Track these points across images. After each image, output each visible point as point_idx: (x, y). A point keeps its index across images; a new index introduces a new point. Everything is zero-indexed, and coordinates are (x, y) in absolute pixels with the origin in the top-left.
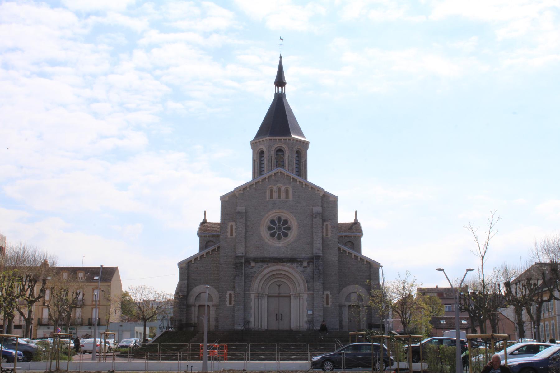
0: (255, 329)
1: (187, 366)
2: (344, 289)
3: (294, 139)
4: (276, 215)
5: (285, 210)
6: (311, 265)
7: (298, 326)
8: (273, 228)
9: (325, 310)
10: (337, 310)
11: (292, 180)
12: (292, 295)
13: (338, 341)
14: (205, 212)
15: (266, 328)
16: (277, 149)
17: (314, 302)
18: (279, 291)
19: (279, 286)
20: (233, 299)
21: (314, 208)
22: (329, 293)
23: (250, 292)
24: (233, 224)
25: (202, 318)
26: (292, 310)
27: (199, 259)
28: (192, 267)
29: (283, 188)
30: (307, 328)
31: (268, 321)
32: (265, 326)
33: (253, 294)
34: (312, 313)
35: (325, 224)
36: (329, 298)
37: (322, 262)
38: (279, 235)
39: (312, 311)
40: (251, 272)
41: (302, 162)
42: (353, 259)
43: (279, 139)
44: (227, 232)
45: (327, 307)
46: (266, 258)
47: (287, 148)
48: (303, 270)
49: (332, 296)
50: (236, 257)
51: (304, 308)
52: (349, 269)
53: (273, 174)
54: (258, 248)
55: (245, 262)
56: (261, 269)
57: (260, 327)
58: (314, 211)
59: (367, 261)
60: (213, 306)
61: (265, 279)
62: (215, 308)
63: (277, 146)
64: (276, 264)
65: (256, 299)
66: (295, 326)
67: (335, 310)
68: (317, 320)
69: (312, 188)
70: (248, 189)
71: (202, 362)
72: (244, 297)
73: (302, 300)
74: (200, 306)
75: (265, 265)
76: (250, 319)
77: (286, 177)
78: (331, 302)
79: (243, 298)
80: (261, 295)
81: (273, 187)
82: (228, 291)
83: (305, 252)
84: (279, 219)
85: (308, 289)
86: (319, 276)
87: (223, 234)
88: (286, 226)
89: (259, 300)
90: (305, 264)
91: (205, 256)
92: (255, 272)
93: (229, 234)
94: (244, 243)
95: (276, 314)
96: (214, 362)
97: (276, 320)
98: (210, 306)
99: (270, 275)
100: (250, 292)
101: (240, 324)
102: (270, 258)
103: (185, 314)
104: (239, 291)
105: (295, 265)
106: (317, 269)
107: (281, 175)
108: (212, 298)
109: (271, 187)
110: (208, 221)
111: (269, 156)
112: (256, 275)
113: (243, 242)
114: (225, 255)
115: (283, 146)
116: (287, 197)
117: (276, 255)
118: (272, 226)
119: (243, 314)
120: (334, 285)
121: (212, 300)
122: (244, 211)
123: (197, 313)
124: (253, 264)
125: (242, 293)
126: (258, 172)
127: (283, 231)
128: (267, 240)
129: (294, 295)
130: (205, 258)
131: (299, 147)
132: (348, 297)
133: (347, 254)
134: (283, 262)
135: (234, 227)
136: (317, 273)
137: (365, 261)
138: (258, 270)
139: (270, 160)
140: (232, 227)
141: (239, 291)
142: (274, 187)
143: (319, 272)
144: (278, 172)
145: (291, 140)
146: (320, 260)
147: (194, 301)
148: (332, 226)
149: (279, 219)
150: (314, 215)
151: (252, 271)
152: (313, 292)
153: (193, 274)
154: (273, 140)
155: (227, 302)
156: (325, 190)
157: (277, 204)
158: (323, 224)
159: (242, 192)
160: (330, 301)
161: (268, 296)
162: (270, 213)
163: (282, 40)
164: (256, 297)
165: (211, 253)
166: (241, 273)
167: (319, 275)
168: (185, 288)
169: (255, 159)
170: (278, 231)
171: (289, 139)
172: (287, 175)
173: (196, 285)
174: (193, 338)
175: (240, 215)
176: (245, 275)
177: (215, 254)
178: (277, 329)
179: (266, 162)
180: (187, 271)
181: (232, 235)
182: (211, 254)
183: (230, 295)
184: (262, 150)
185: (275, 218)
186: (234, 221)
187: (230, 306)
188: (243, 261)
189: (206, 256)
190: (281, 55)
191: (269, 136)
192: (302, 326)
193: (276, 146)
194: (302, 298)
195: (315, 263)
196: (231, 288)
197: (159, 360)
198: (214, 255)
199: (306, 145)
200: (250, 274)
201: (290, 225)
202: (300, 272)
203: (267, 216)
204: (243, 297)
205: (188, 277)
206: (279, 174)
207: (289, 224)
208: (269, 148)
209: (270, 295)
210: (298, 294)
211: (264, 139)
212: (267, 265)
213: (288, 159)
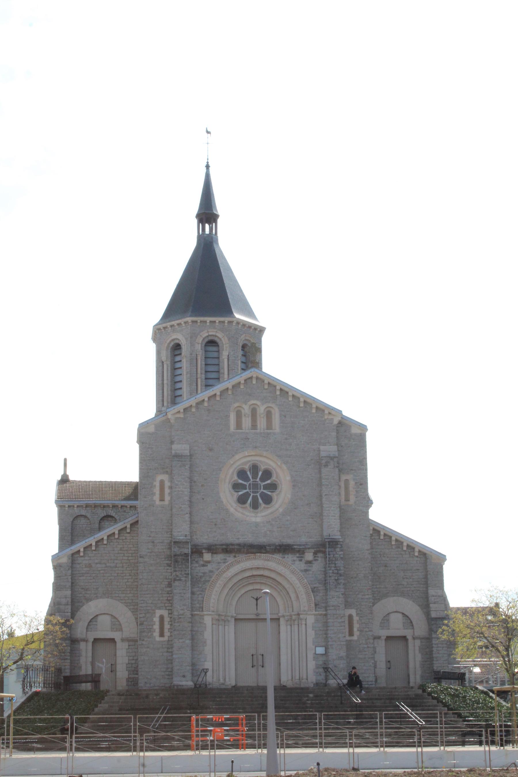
1: (232, 762)
2: (376, 605)
3: (239, 322)
4: (250, 461)
5: (267, 451)
6: (320, 559)
7: (297, 677)
8: (244, 487)
9: (349, 645)
10: (369, 646)
11: (278, 393)
12: (283, 616)
13: (403, 706)
14: (65, 460)
15: (233, 684)
16: (206, 340)
17: (327, 630)
18: (257, 610)
19: (257, 599)
20: (167, 626)
21: (322, 448)
22: (353, 612)
23: (202, 611)
24: (165, 477)
25: (100, 665)
26: (283, 646)
27: (93, 548)
28: (79, 564)
29: (261, 410)
30: (315, 682)
31: (236, 670)
32: (231, 682)
33: (207, 615)
34: (324, 652)
35: (344, 477)
36: (355, 622)
37: (342, 553)
38: (255, 499)
39: (324, 648)
40: (204, 573)
42: (394, 547)
44: (154, 494)
45: (350, 641)
46: (232, 545)
47: (226, 338)
48: (306, 568)
49: (360, 619)
50: (175, 542)
51: (308, 641)
52: (386, 566)
53: (243, 382)
54: (216, 524)
55: (192, 553)
56: (223, 567)
58: (323, 454)
59: (420, 551)
60: (123, 640)
61: (230, 585)
62: (126, 645)
63: (207, 334)
64: (252, 556)
66: (290, 678)
67: (366, 646)
68: (335, 666)
69: (317, 408)
70: (194, 410)
71: (265, 751)
72: (191, 622)
73: (304, 626)
74: (96, 640)
75: (230, 559)
77: (266, 387)
78: (358, 630)
79: (190, 625)
80: (223, 618)
81: (242, 407)
82: (157, 611)
83: (308, 532)
84: (255, 468)
85: (316, 605)
86: (336, 580)
87: (145, 497)
88: (269, 482)
89: (220, 627)
90: (309, 556)
91: (105, 542)
92: (211, 572)
93: (157, 497)
94: (188, 515)
95: (252, 655)
96: (217, 753)
97: (253, 667)
98: (116, 640)
99: (240, 577)
100: (202, 611)
101: (184, 676)
102: (239, 545)
103: (69, 658)
104: (182, 610)
105: (290, 558)
106: (333, 565)
107: (257, 382)
108: (120, 625)
109: (238, 407)
110: (71, 478)
111: (191, 354)
112: (213, 578)
113: (187, 514)
114: (151, 538)
115: (218, 334)
116: (269, 425)
117: (250, 539)
118: (240, 481)
119: (191, 656)
121: (121, 630)
122: (187, 453)
123: (90, 654)
124: (207, 556)
125: (188, 614)
126: (169, 384)
127: (262, 492)
128: (232, 510)
129: (286, 618)
130: (105, 546)
131: (247, 338)
132: (385, 621)
133: (382, 537)
134: (267, 552)
135: (167, 484)
136: (333, 573)
137: (417, 550)
138: (218, 569)
139: (193, 361)
140: (162, 483)
141: (182, 610)
142: (244, 406)
143: (336, 572)
144: (251, 378)
145: (234, 324)
146: (338, 547)
147: (85, 631)
148: (356, 483)
149: (255, 468)
150: (323, 462)
151: (206, 569)
152: (326, 610)
153: (81, 578)
154: (199, 324)
155: (155, 631)
156: (344, 414)
157: (250, 440)
158: (340, 480)
159: (182, 416)
160: (355, 629)
161: (236, 620)
162: (237, 457)
163: (209, 134)
164: (214, 622)
165: (116, 536)
166: (185, 574)
167: (336, 578)
168: (68, 605)
169: (164, 359)
170: (253, 492)
171: (230, 322)
172: (269, 383)
173: (88, 600)
174: (99, 705)
175: (178, 461)
176: (192, 578)
177: (124, 538)
179: (185, 364)
180: (70, 572)
181: (162, 499)
182: (118, 538)
183: (162, 618)
184: (177, 341)
185: (247, 467)
186: (167, 473)
187: (162, 639)
188: (188, 550)
189: (108, 542)
190: (208, 162)
191: (191, 316)
192: (305, 677)
194: (304, 622)
195: (329, 555)
196: (163, 605)
197: (71, 750)
198: (123, 540)
199: (260, 331)
200: (201, 576)
201: (276, 481)
202: (299, 571)
203: (232, 463)
204: (189, 622)
205: (72, 583)
206: (254, 382)
207: (274, 478)
208: (191, 337)
210: (295, 615)
211: (182, 321)
212: (236, 559)
213: (228, 359)
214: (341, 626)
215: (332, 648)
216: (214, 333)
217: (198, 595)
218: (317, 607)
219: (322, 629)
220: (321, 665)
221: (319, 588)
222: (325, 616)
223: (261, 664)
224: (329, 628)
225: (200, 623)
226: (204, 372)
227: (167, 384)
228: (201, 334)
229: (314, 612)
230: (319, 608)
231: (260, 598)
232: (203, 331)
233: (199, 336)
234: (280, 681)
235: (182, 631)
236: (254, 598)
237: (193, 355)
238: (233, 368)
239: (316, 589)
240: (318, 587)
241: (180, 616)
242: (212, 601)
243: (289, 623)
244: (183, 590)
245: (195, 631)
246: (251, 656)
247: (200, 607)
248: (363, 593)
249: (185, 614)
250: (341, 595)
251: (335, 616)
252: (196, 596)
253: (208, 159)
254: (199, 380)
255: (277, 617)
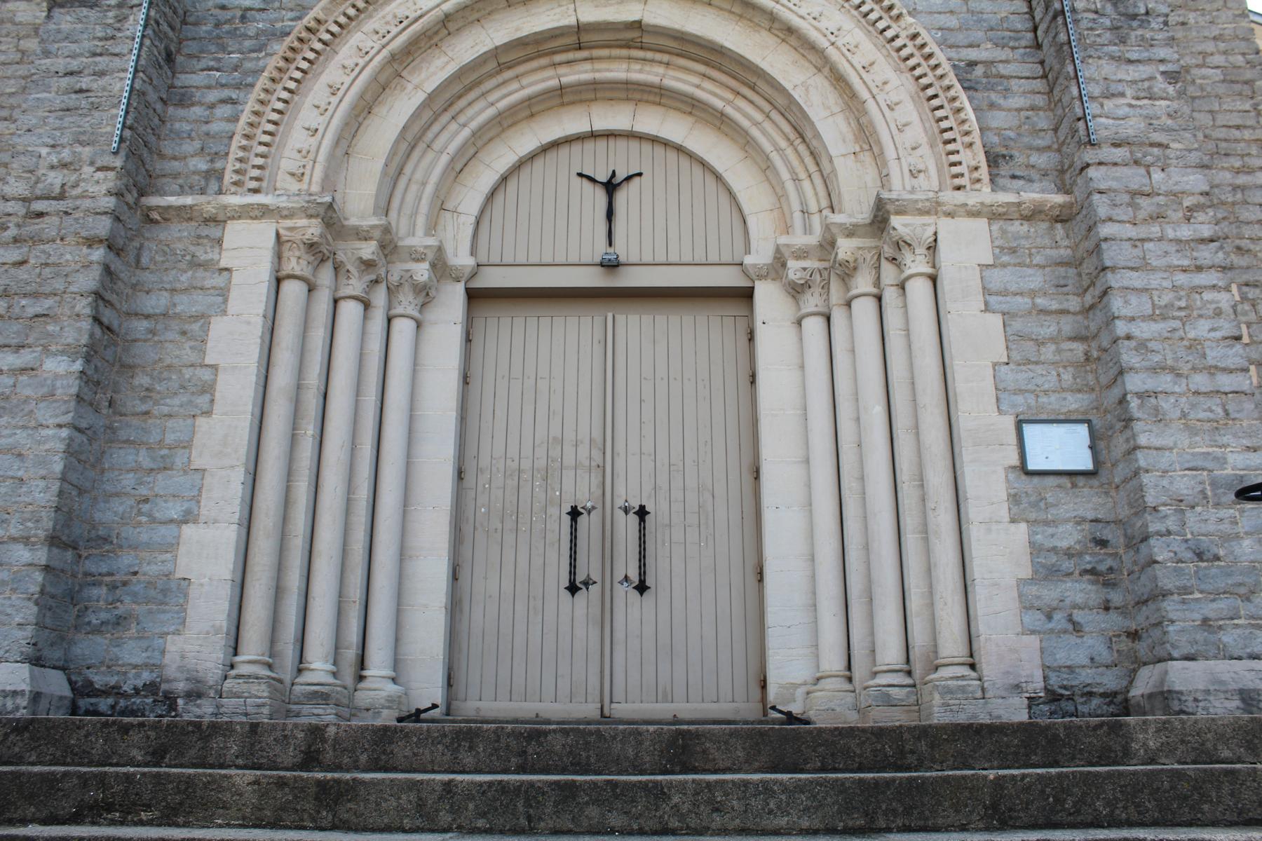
0: (229, 704)
7: (891, 653)
18: (610, 245)
19: (611, 187)
31: (455, 606)
49: (1244, 298)
51: (960, 385)
57: (319, 668)
65: (293, 290)
66: (833, 661)
73: (919, 290)
76: (171, 547)
85: (994, 160)
89: (350, 310)
95: (575, 513)
97: (573, 589)
104: (64, 165)
119: (58, 467)
120: (1242, 180)
161: (475, 296)
178: (589, 710)
192: (952, 645)
209: (493, 279)
210: (851, 232)
214: (1199, 269)
215: (1159, 418)
217: (212, 106)
218: (1005, 170)
219: (1055, 306)
220: (1069, 553)
221: (1003, 69)
222: (1059, 226)
223: (634, 576)
224: (1113, 280)
225: (195, 264)
229: (985, 195)
230: (1014, 177)
231: (629, 178)
234: (764, 685)
235: (35, 295)
236: (592, 180)
239: (979, 70)
240: (989, 63)
241: (39, 206)
242: (297, 138)
243: (812, 302)
244: (95, 55)
245: (147, 317)
246: (567, 519)
247: (208, 175)
248: (1237, 163)
249: (78, 191)
250: (1159, 77)
251: (1143, 201)
252: (197, 111)
255: (742, 282)
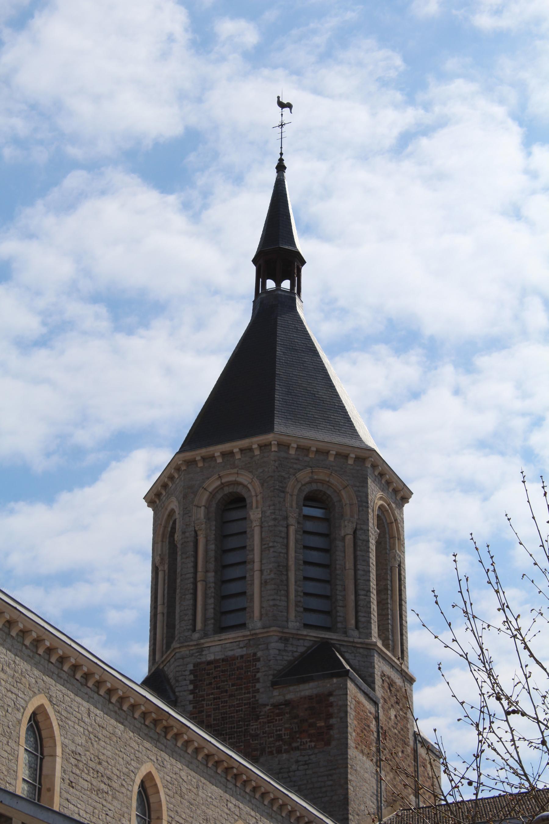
41: (343, 539)
43: (224, 454)
63: (218, 483)
115: (241, 479)
145: (274, 448)
154: (200, 464)
163: (287, 110)
190: (281, 160)
193: (213, 484)
216: (232, 478)
226: (212, 566)
227: (163, 614)
228: (205, 485)
232: (208, 478)
233: (201, 490)
237: (187, 534)
238: (271, 544)
253: (281, 154)
254: (200, 587)
